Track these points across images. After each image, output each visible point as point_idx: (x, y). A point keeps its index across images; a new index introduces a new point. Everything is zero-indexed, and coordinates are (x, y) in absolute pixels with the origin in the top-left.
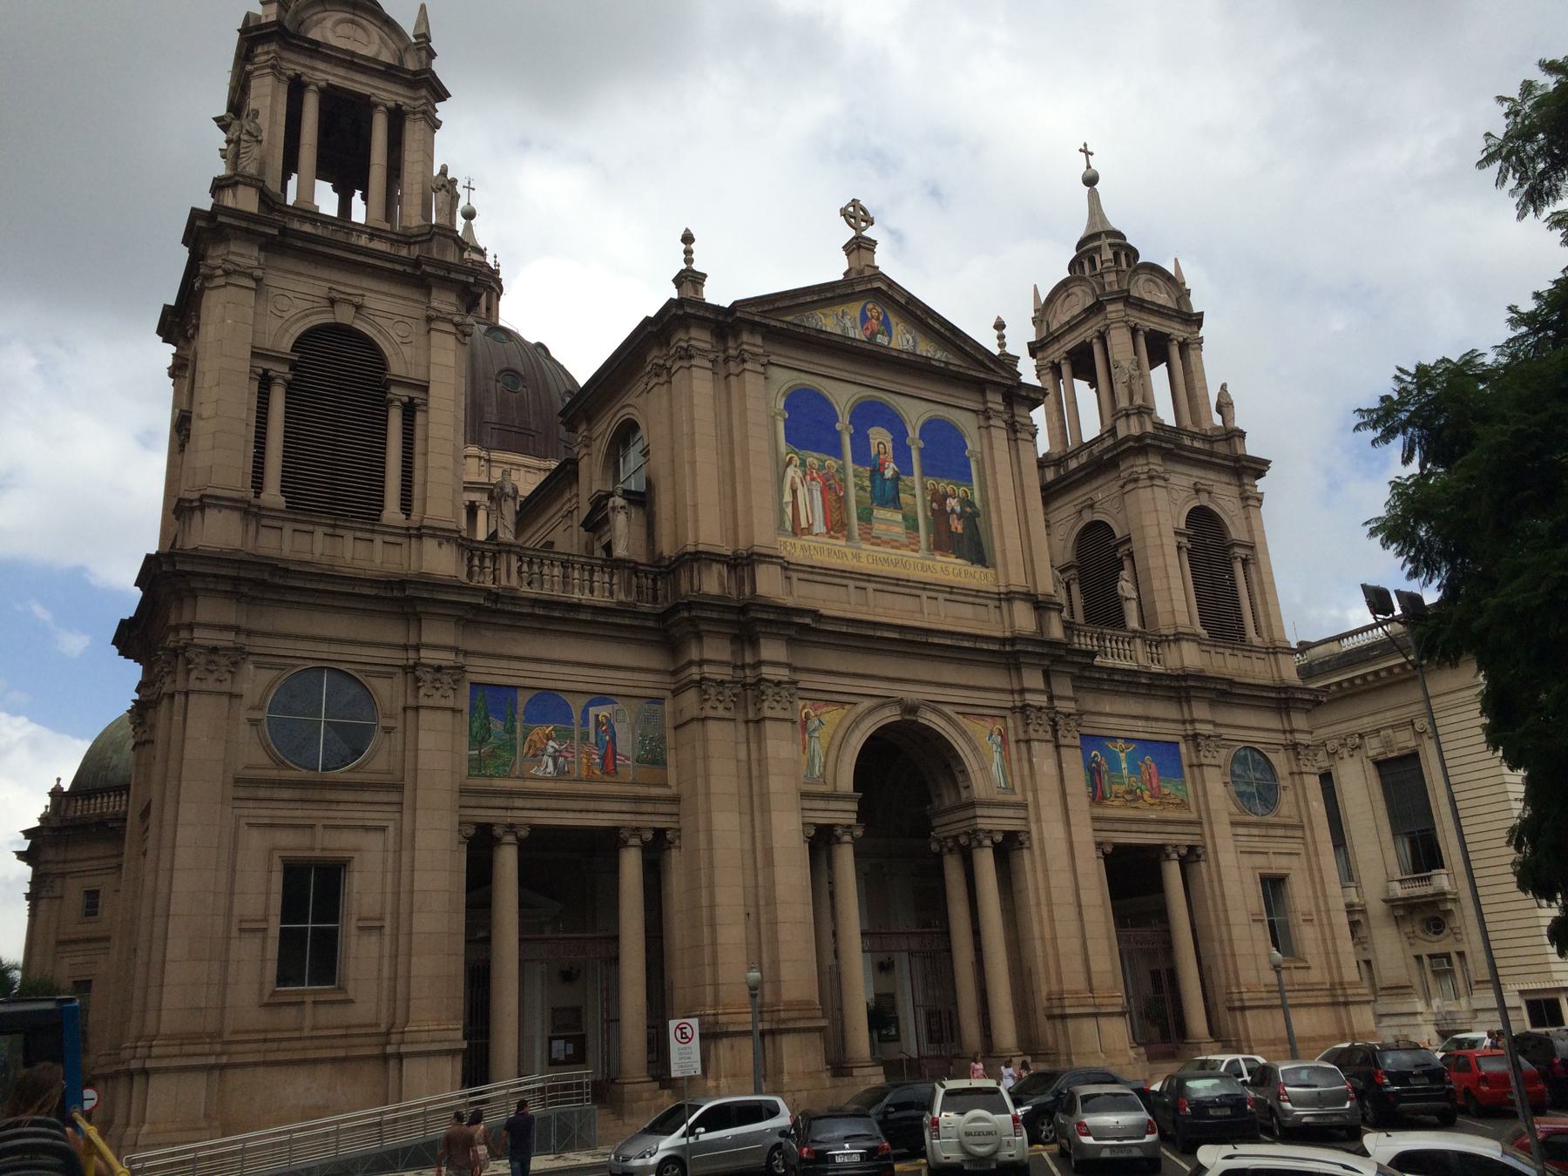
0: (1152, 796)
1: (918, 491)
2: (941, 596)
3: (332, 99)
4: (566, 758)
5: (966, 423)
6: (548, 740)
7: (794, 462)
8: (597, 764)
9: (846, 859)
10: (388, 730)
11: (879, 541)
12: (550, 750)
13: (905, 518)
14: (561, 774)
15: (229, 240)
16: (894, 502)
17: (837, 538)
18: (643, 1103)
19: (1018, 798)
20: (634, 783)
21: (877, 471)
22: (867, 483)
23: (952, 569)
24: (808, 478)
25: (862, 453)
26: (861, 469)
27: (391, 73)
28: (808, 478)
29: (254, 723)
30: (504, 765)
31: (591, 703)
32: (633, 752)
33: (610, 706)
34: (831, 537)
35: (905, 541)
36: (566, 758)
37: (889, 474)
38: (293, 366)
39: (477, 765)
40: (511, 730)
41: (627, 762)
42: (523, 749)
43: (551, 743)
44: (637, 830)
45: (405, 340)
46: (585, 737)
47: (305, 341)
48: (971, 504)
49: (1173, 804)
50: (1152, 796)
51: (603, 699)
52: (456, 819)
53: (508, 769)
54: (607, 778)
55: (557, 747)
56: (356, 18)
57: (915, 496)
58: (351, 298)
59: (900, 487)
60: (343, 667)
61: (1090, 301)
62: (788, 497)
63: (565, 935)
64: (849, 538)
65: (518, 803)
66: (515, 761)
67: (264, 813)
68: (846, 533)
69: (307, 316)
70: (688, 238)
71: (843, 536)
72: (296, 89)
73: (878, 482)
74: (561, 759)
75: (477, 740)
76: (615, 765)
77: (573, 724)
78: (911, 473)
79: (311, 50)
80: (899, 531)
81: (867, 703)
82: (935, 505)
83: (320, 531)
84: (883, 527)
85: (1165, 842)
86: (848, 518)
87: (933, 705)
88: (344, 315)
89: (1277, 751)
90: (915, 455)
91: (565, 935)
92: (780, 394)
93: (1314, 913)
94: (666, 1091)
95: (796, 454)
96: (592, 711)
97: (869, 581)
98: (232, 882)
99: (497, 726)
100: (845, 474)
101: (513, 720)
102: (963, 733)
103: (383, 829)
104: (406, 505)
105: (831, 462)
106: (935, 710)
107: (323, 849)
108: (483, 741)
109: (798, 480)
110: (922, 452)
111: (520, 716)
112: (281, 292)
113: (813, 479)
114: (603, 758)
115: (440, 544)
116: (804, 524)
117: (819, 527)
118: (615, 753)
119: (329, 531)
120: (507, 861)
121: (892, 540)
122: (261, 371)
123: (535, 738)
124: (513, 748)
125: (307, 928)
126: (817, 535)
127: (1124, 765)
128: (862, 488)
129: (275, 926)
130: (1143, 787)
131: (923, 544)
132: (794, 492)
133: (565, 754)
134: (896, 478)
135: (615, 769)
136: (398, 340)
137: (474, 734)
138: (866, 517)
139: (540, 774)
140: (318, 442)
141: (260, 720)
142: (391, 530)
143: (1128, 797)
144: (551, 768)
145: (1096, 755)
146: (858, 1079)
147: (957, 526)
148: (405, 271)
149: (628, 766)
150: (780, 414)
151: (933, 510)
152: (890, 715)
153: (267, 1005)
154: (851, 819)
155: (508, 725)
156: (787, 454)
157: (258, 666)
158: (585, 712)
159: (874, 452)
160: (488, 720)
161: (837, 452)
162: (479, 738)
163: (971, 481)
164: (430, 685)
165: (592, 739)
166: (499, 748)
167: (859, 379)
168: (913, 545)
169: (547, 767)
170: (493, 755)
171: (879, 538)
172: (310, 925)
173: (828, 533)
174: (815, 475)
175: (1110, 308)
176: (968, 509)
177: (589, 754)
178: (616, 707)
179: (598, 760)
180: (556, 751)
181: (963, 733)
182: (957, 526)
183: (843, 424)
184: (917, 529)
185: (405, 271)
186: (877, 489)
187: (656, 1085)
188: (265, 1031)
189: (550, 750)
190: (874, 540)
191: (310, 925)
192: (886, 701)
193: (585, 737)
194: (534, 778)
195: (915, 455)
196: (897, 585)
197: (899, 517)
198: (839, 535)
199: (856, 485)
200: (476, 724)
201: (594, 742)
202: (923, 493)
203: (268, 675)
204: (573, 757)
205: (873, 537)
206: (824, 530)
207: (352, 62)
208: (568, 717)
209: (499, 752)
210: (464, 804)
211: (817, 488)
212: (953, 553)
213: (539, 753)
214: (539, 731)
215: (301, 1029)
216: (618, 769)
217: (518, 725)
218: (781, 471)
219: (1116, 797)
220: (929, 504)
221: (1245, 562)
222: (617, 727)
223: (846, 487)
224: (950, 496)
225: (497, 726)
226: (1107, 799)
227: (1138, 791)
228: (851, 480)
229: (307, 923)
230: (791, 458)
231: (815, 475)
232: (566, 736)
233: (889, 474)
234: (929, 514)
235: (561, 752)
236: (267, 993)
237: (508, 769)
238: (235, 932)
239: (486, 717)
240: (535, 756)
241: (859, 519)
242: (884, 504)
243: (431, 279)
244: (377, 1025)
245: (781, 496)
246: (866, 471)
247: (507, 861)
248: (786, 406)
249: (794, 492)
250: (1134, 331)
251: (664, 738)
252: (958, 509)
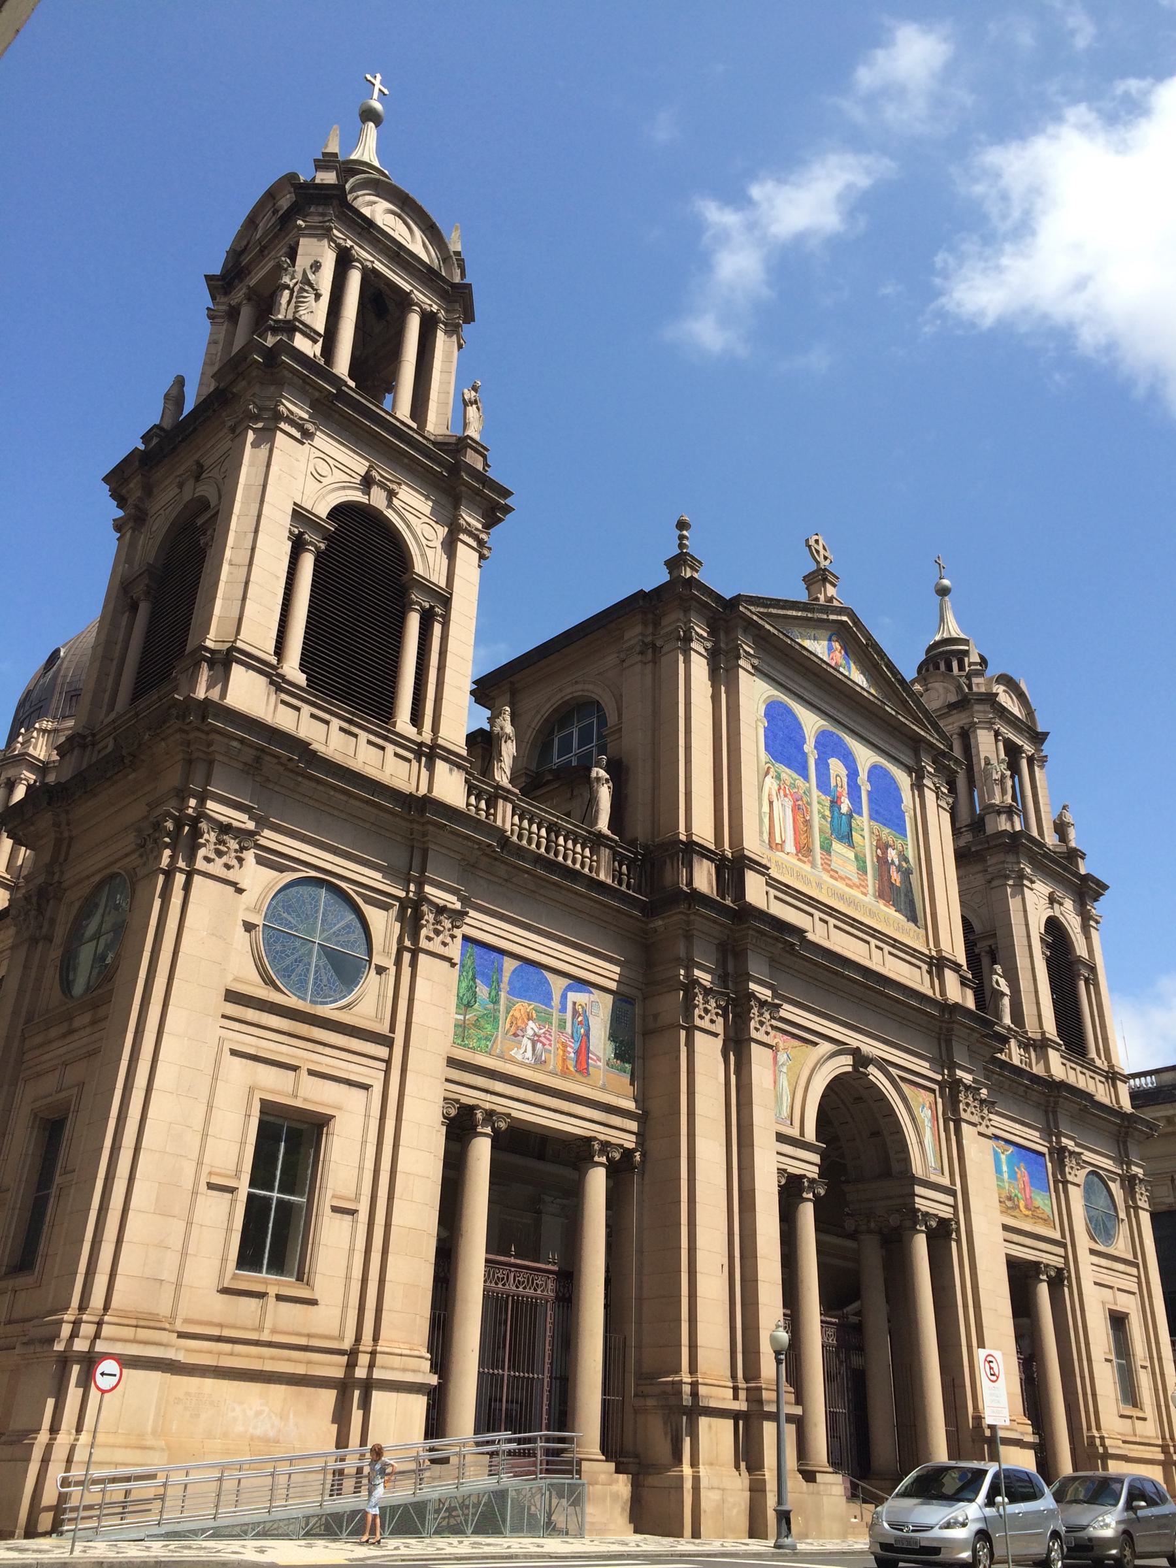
2: (887, 948)
3: (372, 284)
4: (544, 1045)
5: (903, 780)
6: (529, 1020)
7: (771, 773)
8: (571, 1059)
9: (807, 1214)
10: (380, 970)
11: (836, 875)
12: (530, 1032)
13: (856, 857)
15: (283, 385)
16: (847, 838)
17: (804, 862)
18: (598, 1487)
19: (946, 1181)
20: (603, 1089)
21: (835, 803)
22: (827, 813)
23: (889, 919)
24: (782, 792)
25: (824, 784)
26: (823, 797)
27: (427, 276)
28: (782, 792)
29: (249, 927)
30: (487, 1039)
31: (569, 988)
32: (604, 1054)
33: (587, 994)
34: (799, 860)
35: (856, 881)
36: (544, 1045)
37: (844, 809)
38: (327, 537)
39: (462, 1031)
40: (495, 1001)
41: (599, 1063)
42: (504, 1024)
43: (531, 1024)
44: (606, 1146)
45: (430, 544)
46: (562, 1024)
47: (340, 512)
48: (906, 860)
51: (582, 984)
52: (443, 1094)
53: (490, 1044)
54: (577, 1075)
55: (536, 1030)
56: (403, 214)
57: (864, 837)
58: (388, 483)
59: (853, 825)
60: (343, 885)
61: (953, 698)
62: (766, 808)
63: (518, 1261)
64: (813, 866)
65: (499, 1087)
66: (497, 1037)
67: (249, 1043)
68: (810, 858)
69: (344, 488)
70: (682, 525)
71: (809, 861)
72: (344, 261)
73: (836, 814)
74: (539, 1046)
75: (466, 1003)
76: (588, 1064)
77: (552, 1008)
78: (861, 814)
79: (363, 228)
80: (851, 870)
81: (826, 1047)
82: (879, 851)
83: (336, 723)
84: (840, 862)
85: (1040, 1260)
86: (813, 844)
87: (883, 1065)
88: (378, 498)
89: (1114, 1181)
91: (518, 1261)
92: (762, 700)
94: (621, 1476)
95: (773, 765)
96: (572, 996)
97: (830, 915)
98: (207, 1121)
99: (483, 991)
100: (810, 797)
101: (498, 990)
102: (904, 1099)
103: (366, 1087)
104: (416, 719)
105: (800, 782)
107: (305, 1100)
108: (468, 1005)
109: (774, 793)
110: (869, 793)
111: (505, 985)
112: (323, 456)
113: (786, 795)
114: (577, 1053)
115: (451, 770)
116: (778, 841)
117: (790, 847)
118: (588, 1051)
119: (345, 725)
120: (482, 1151)
121: (847, 877)
122: (297, 532)
123: (517, 1014)
124: (496, 1019)
125: (279, 1192)
126: (788, 854)
128: (824, 817)
129: (244, 1189)
130: (1019, 1195)
131: (870, 889)
132: (771, 803)
133: (542, 1039)
134: (850, 816)
135: (587, 1069)
136: (424, 542)
137: (461, 995)
138: (827, 849)
140: (344, 624)
141: (255, 926)
142: (400, 741)
143: (1009, 1204)
144: (529, 1054)
146: (822, 1487)
147: (896, 877)
148: (441, 472)
149: (598, 1067)
150: (760, 720)
151: (878, 856)
153: (225, 1291)
154: (812, 1172)
155: (493, 993)
156: (766, 763)
157: (260, 861)
158: (564, 997)
159: (833, 783)
160: (475, 983)
161: (803, 772)
162: (465, 1002)
163: (906, 836)
164: (432, 927)
165: (569, 1029)
166: (482, 1017)
167: (824, 706)
168: (862, 886)
169: (525, 1051)
170: (477, 1025)
171: (837, 872)
172: (275, 1195)
173: (797, 855)
174: (787, 792)
175: (977, 707)
176: (904, 864)
177: (565, 1046)
178: (593, 998)
179: (572, 1055)
180: (535, 1034)
181: (904, 1099)
182: (896, 877)
183: (809, 747)
184: (865, 873)
185: (441, 472)
186: (836, 820)
187: (612, 1466)
188: (221, 1326)
189: (530, 1032)
190: (832, 873)
191: (275, 1195)
192: (842, 1049)
193: (562, 1024)
194: (513, 1061)
196: (852, 926)
197: (851, 855)
198: (805, 859)
199: (819, 812)
200: (464, 985)
201: (570, 1032)
202: (871, 837)
203: (269, 874)
204: (550, 1045)
205: (832, 870)
206: (793, 851)
207: (397, 254)
208: (547, 998)
209: (482, 1022)
210: (450, 1077)
211: (789, 803)
212: (893, 905)
213: (519, 1033)
214: (522, 1007)
215: (260, 1329)
216: (591, 1069)
217: (503, 995)
218: (761, 780)
220: (874, 848)
221: (1087, 980)
222: (591, 1019)
223: (811, 812)
224: (890, 846)
225: (483, 991)
228: (816, 807)
229: (272, 1190)
230: (769, 768)
231: (787, 792)
232: (544, 1020)
233: (844, 809)
234: (875, 860)
235: (539, 1036)
236: (229, 1275)
237: (490, 1044)
238: (203, 1187)
239: (474, 979)
240: (515, 1035)
241: (822, 848)
242: (840, 839)
243: (464, 488)
244: (341, 1338)
245: (760, 805)
246: (827, 801)
247: (482, 1151)
248: (766, 715)
249: (771, 803)
250: (997, 734)
251: (633, 1043)
252: (897, 863)
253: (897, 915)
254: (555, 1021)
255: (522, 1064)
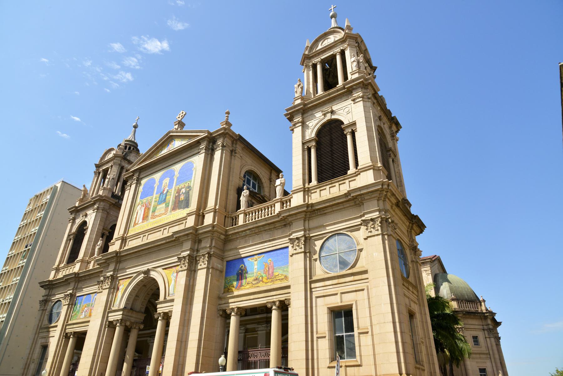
0: (268, 279)
1: (172, 194)
4: (87, 312)
12: (85, 310)
14: (85, 316)
42: (80, 311)
43: (86, 308)
49: (279, 279)
50: (268, 279)
65: (75, 326)
90: (175, 180)
93: (370, 327)
106: (154, 271)
109: (139, 209)
127: (256, 267)
130: (264, 275)
133: (87, 311)
139: (81, 317)
143: (254, 282)
145: (242, 266)
152: (141, 276)
170: (75, 314)
189: (85, 310)
192: (139, 273)
195: (175, 180)
219: (248, 284)
226: (243, 286)
227: (261, 278)
246: (158, 195)
253: (180, 210)
254: (90, 306)
255: (82, 318)
